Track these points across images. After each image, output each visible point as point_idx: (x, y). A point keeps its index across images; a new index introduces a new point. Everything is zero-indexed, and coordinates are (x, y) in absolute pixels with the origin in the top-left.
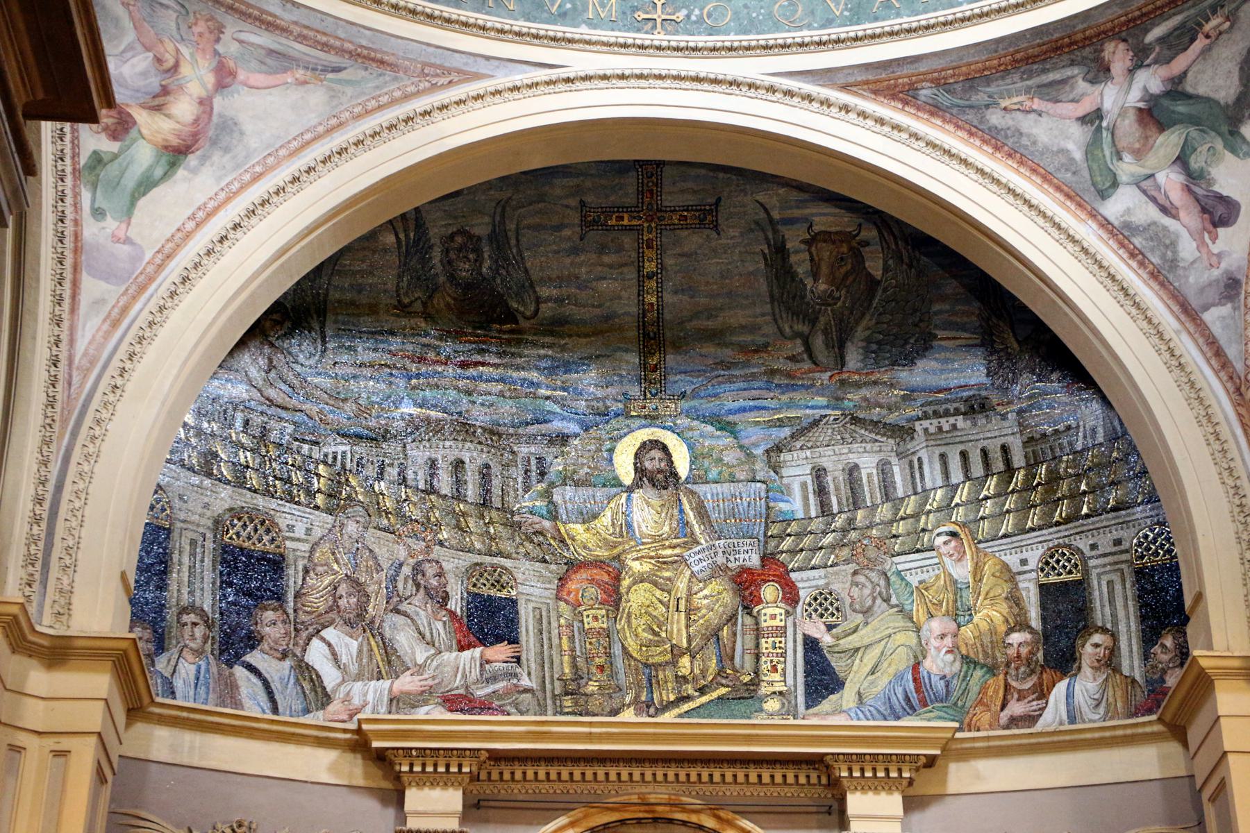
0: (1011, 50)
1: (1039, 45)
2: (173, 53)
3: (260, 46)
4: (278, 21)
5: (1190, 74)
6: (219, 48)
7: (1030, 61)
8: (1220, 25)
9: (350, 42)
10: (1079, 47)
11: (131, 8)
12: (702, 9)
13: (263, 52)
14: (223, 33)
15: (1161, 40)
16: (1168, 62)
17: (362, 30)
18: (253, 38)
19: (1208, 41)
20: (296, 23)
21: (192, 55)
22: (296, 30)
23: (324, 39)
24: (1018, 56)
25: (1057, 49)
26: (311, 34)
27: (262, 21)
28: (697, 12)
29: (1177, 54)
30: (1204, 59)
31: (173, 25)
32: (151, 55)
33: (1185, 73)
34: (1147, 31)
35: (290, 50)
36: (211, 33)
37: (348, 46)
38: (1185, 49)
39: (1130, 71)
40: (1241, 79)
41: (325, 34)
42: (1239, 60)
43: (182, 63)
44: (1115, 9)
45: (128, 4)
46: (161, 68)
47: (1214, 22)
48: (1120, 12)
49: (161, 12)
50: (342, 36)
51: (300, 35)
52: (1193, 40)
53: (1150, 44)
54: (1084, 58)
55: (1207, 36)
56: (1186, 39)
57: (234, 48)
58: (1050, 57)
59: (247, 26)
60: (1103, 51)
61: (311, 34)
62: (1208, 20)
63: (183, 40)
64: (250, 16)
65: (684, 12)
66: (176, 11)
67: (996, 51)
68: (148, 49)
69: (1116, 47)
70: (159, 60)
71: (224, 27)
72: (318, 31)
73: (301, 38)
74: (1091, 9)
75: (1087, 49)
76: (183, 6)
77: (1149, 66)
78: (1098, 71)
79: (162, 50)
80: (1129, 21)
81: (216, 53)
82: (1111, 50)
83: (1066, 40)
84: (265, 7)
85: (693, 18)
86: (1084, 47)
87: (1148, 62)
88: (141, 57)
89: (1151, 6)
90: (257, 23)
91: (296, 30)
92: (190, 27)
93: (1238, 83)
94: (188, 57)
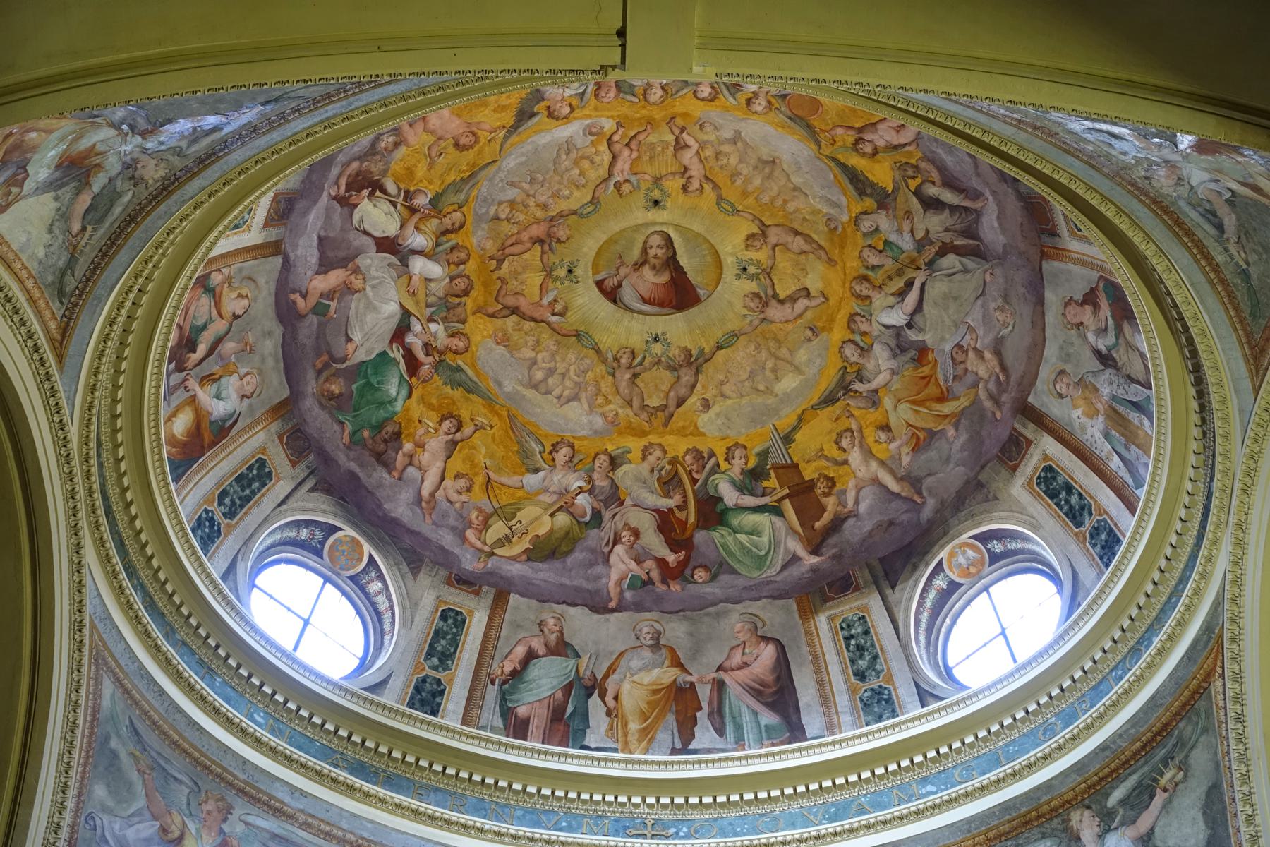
0: (983, 828)
1: (1009, 822)
2: (180, 826)
3: (264, 830)
4: (285, 808)
5: (1157, 830)
6: (226, 827)
7: (1003, 838)
8: (1174, 777)
9: (352, 833)
10: (1047, 820)
11: (146, 776)
12: (689, 828)
13: (267, 836)
14: (231, 814)
15: (1123, 802)
16: (1134, 822)
17: (364, 822)
18: (260, 822)
19: (1167, 795)
20: (302, 811)
21: (198, 831)
22: (302, 817)
23: (328, 829)
24: (991, 835)
25: (1027, 823)
26: (315, 823)
27: (269, 807)
28: (685, 829)
29: (1140, 813)
30: (1167, 812)
31: (184, 800)
32: (158, 824)
33: (1152, 830)
34: (1107, 795)
35: (293, 836)
36: (219, 812)
37: (349, 836)
38: (1148, 807)
39: (1100, 836)
40: (1206, 823)
41: (328, 824)
42: (1200, 806)
43: (187, 836)
44: (1074, 776)
45: (144, 773)
46: (165, 838)
47: (1168, 775)
48: (1080, 779)
49: (174, 785)
50: (345, 827)
51: (304, 823)
52: (1152, 797)
53: (1113, 807)
54: (1053, 830)
55: (1165, 790)
56: (1146, 797)
57: (240, 828)
58: (1022, 833)
59: (254, 810)
60: (1070, 820)
61: (315, 823)
62: (1162, 774)
63: (191, 815)
64: (259, 800)
65: (673, 830)
66: (188, 787)
67: (969, 831)
68: (155, 818)
69: (1082, 815)
70: (164, 830)
71: (232, 808)
72: (322, 821)
73: (306, 826)
74: (1052, 779)
75: (1055, 820)
76: (196, 784)
77: (1116, 829)
78: (1070, 841)
79: (169, 821)
80: (1089, 788)
81: (221, 831)
82: (1078, 818)
83: (1034, 813)
84: (275, 794)
85: (682, 834)
86: (1051, 819)
87: (1114, 825)
88: (147, 824)
89: (1107, 769)
90: (265, 808)
91: (302, 817)
92: (200, 804)
93: (1204, 827)
94: (193, 831)
